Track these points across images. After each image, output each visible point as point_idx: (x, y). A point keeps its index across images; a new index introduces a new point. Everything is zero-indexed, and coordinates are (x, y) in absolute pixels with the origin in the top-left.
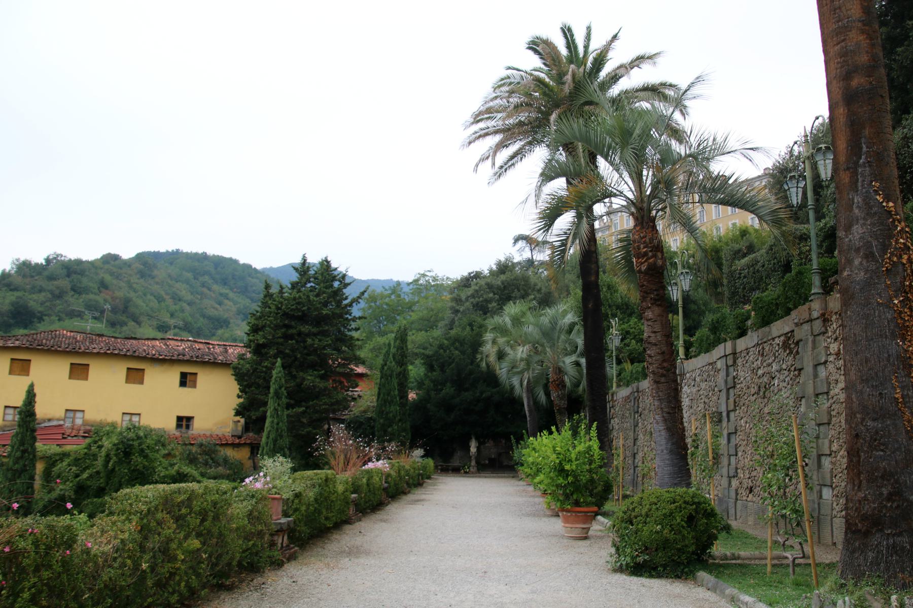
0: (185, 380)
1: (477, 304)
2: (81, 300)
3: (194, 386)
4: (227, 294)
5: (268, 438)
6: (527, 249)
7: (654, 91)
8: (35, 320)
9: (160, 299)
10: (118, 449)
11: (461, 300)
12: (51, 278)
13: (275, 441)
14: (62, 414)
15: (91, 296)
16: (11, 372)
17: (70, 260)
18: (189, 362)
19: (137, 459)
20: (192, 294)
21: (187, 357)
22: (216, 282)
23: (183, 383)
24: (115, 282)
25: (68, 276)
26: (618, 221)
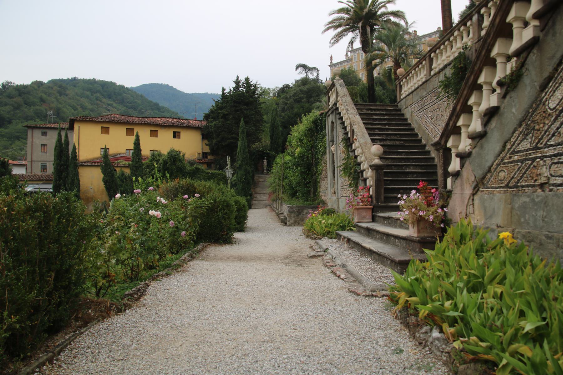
0: (176, 135)
1: (296, 99)
2: (32, 110)
3: (179, 138)
4: (112, 104)
5: (240, 149)
6: (304, 72)
7: (396, 14)
8: (6, 123)
9: (75, 109)
10: (171, 159)
11: (287, 98)
12: (10, 97)
13: (244, 150)
14: (124, 151)
15: (38, 107)
16: (102, 133)
17: (17, 85)
18: (177, 127)
19: (178, 163)
20: (92, 104)
21: (176, 124)
22: (105, 97)
23: (174, 137)
24: (49, 98)
25: (20, 95)
26: (356, 56)
